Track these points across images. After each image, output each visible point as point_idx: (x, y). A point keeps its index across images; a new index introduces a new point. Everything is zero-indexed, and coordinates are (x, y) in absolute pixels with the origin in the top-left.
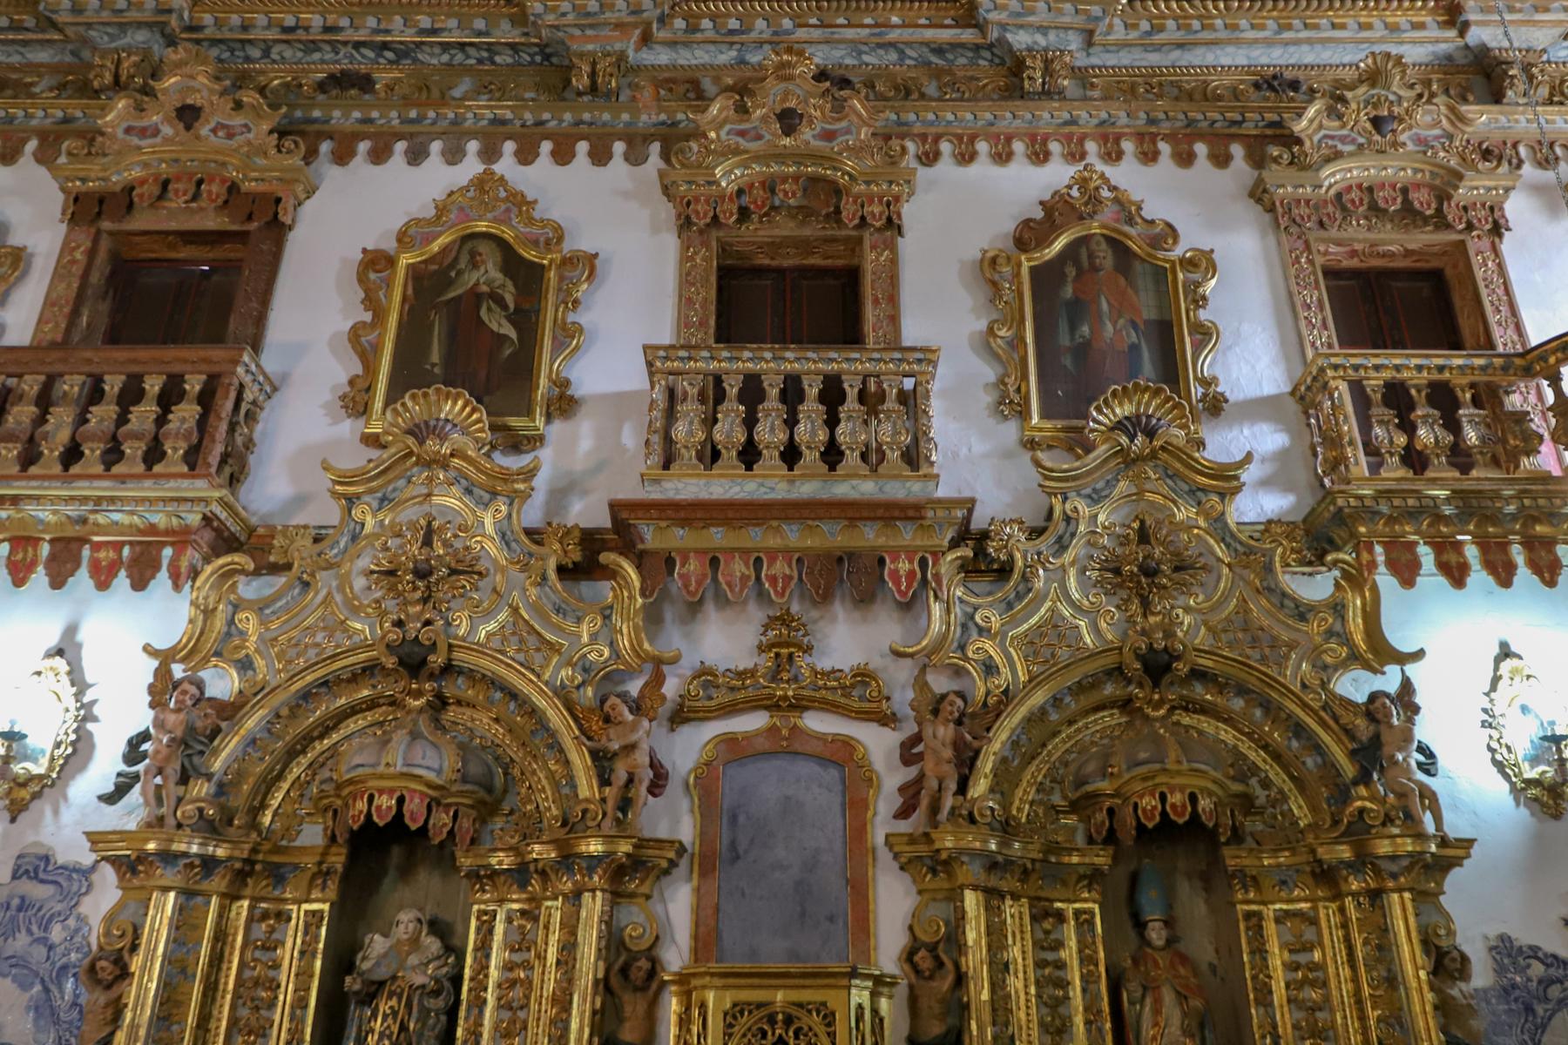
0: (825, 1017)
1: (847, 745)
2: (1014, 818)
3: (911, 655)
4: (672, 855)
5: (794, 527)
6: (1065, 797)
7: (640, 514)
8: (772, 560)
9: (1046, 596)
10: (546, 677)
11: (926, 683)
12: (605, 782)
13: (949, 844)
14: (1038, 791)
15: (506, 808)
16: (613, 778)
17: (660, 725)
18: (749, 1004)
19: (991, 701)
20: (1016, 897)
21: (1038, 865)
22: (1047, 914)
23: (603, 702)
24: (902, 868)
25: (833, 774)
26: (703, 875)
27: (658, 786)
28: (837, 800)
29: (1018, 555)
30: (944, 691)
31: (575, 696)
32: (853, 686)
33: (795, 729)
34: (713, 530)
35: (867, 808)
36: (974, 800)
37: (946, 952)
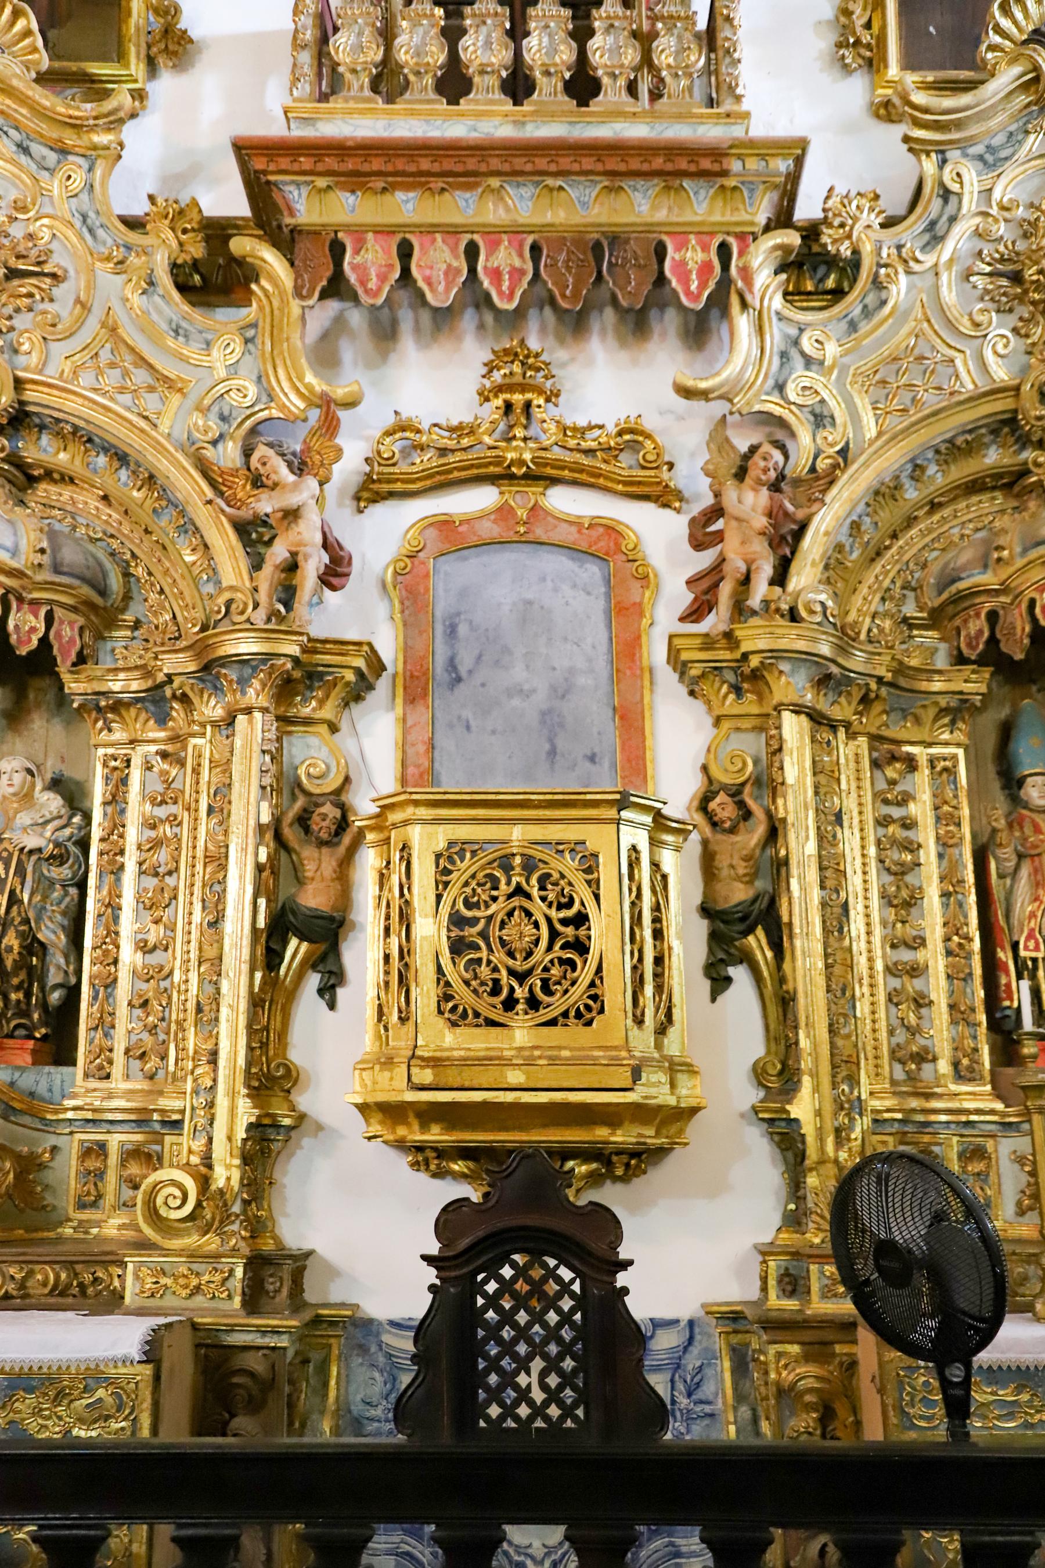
1: (612, 530)
9: (907, 313)
10: (164, 428)
11: (727, 440)
19: (822, 464)
22: (893, 758)
25: (592, 571)
28: (601, 603)
29: (867, 249)
31: (209, 453)
33: (535, 509)
35: (641, 615)
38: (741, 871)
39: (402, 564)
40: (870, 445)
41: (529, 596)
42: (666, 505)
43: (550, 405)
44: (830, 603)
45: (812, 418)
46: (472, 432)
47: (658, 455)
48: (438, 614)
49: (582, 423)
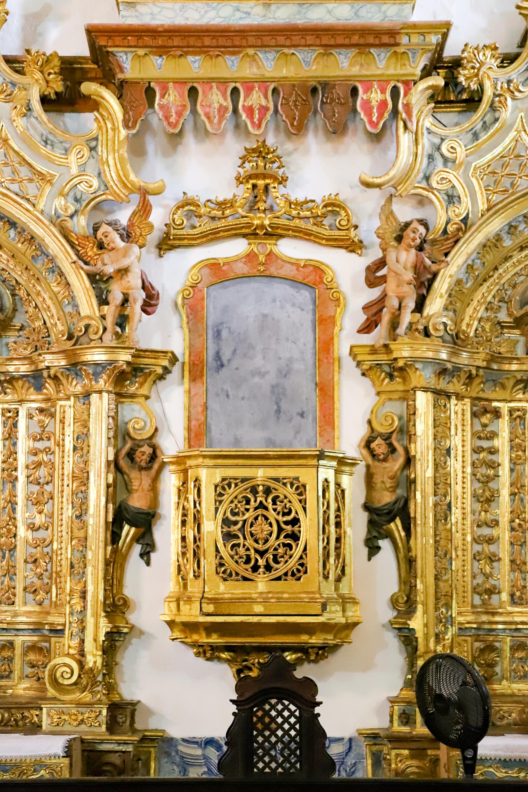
0: (297, 488)
2: (464, 332)
3: (379, 186)
4: (166, 363)
5: (271, 55)
6: (510, 315)
7: (118, 40)
8: (249, 90)
9: (511, 126)
10: (41, 206)
11: (392, 212)
12: (103, 301)
13: (406, 354)
14: (487, 309)
15: (17, 322)
16: (110, 298)
17: (148, 252)
18: (236, 479)
19: (451, 229)
20: (459, 397)
21: (481, 372)
22: (486, 411)
23: (96, 229)
24: (363, 374)
25: (305, 295)
26: (193, 379)
27: (151, 305)
28: (310, 317)
30: (408, 219)
32: (324, 216)
33: (270, 255)
34: (190, 58)
35: (334, 324)
36: (429, 317)
37: (398, 441)
38: (388, 485)
39: (188, 292)
40: (482, 215)
41: (266, 311)
42: (353, 251)
43: (281, 186)
44: (449, 323)
45: (446, 198)
46: (232, 206)
47: (348, 220)
48: (210, 323)
49: (301, 199)
